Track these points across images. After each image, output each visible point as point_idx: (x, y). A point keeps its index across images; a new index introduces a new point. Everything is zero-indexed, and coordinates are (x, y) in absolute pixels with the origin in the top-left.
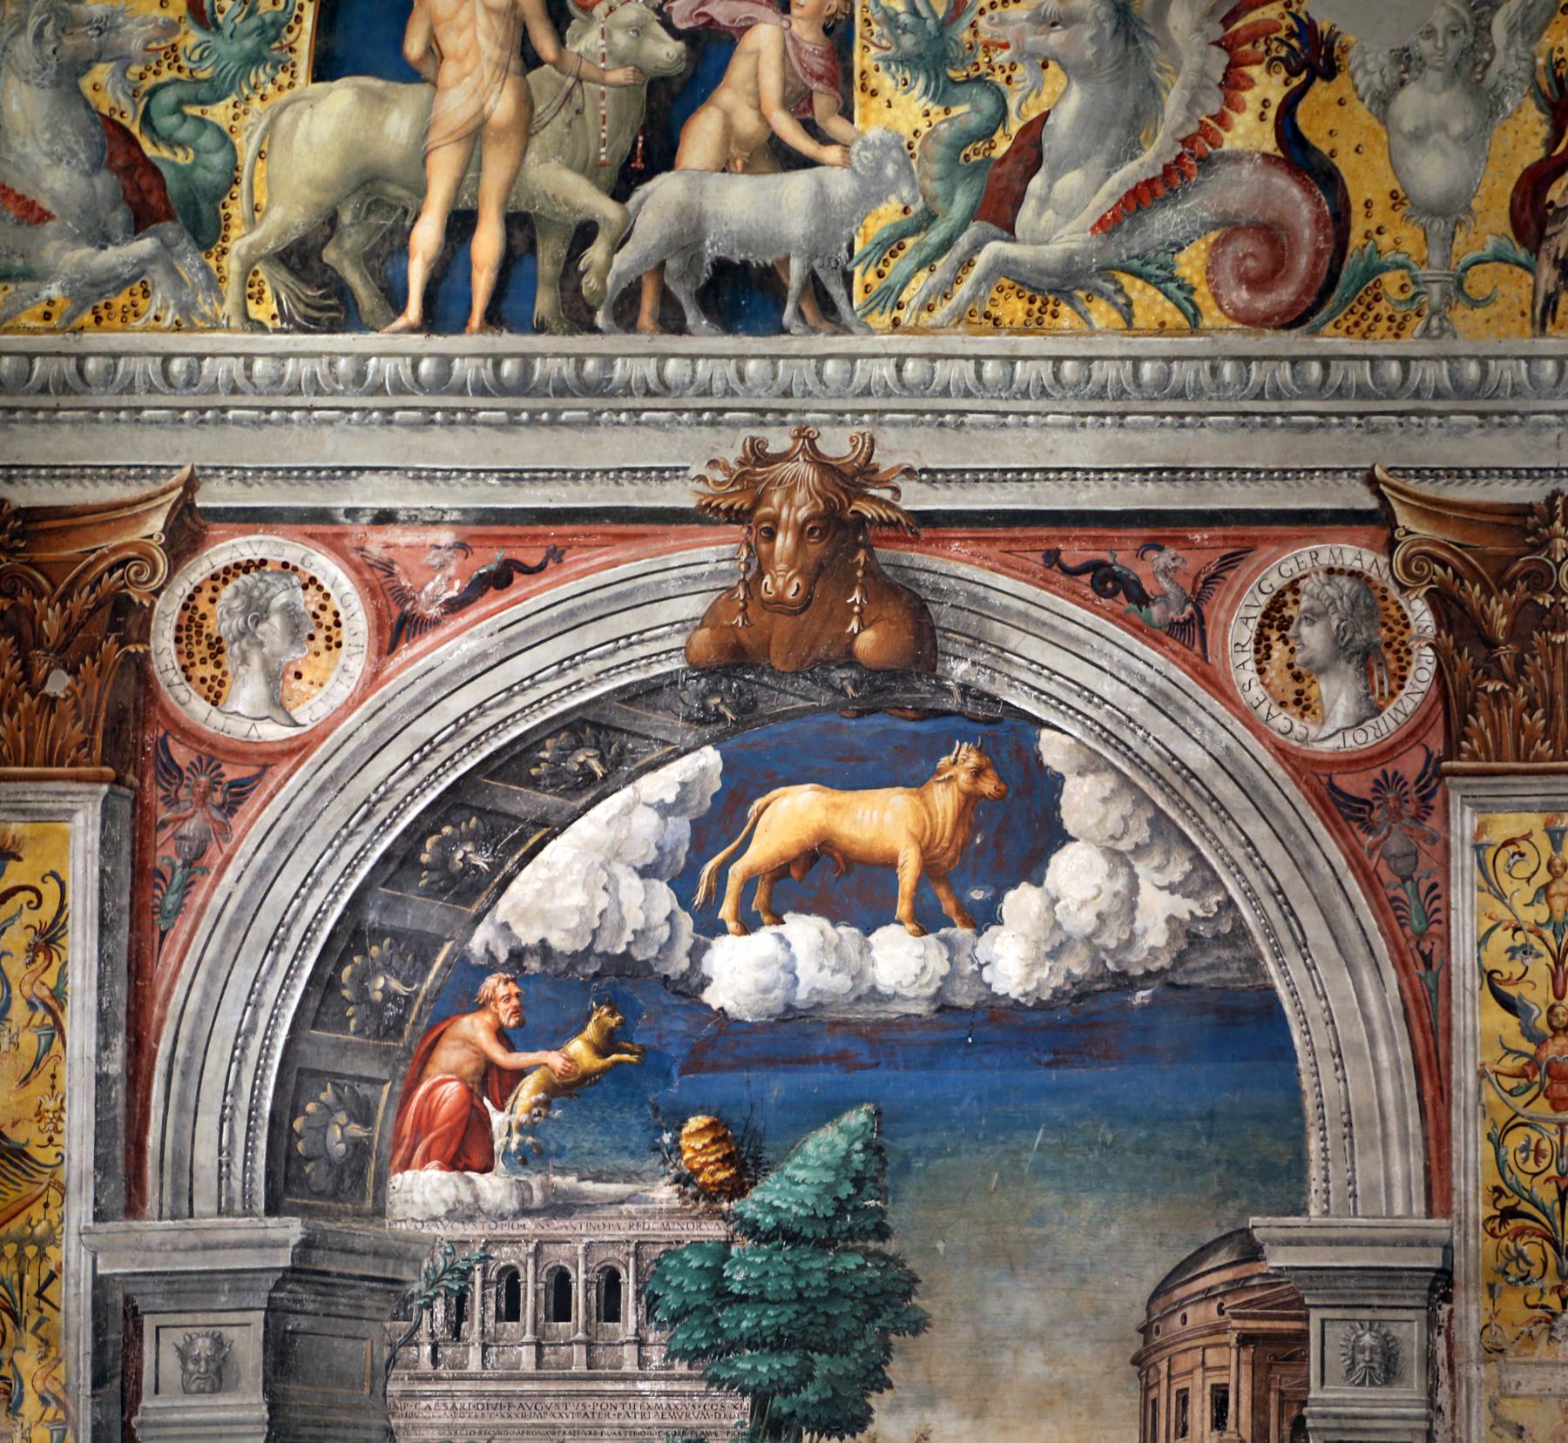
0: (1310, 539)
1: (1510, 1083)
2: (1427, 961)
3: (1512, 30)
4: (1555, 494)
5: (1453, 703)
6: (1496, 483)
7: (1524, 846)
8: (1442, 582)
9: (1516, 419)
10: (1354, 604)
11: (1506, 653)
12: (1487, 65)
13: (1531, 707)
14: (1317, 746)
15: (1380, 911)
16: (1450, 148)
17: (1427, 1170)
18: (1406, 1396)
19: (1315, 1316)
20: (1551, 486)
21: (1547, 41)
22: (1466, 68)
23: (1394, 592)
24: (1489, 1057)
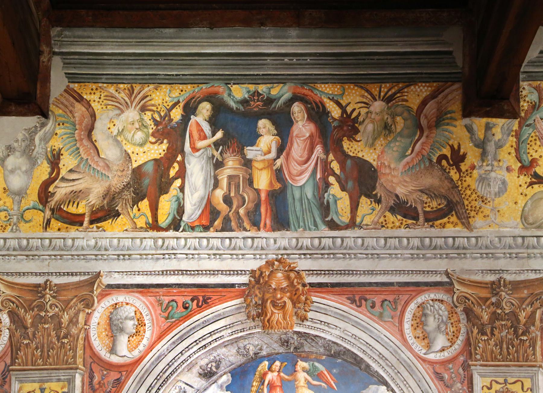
3: (41, 140)
4: (47, 281)
6: (30, 277)
8: (12, 308)
9: (37, 257)
12: (33, 150)
16: (22, 175)
20: (46, 278)
21: (50, 143)
22: (27, 151)
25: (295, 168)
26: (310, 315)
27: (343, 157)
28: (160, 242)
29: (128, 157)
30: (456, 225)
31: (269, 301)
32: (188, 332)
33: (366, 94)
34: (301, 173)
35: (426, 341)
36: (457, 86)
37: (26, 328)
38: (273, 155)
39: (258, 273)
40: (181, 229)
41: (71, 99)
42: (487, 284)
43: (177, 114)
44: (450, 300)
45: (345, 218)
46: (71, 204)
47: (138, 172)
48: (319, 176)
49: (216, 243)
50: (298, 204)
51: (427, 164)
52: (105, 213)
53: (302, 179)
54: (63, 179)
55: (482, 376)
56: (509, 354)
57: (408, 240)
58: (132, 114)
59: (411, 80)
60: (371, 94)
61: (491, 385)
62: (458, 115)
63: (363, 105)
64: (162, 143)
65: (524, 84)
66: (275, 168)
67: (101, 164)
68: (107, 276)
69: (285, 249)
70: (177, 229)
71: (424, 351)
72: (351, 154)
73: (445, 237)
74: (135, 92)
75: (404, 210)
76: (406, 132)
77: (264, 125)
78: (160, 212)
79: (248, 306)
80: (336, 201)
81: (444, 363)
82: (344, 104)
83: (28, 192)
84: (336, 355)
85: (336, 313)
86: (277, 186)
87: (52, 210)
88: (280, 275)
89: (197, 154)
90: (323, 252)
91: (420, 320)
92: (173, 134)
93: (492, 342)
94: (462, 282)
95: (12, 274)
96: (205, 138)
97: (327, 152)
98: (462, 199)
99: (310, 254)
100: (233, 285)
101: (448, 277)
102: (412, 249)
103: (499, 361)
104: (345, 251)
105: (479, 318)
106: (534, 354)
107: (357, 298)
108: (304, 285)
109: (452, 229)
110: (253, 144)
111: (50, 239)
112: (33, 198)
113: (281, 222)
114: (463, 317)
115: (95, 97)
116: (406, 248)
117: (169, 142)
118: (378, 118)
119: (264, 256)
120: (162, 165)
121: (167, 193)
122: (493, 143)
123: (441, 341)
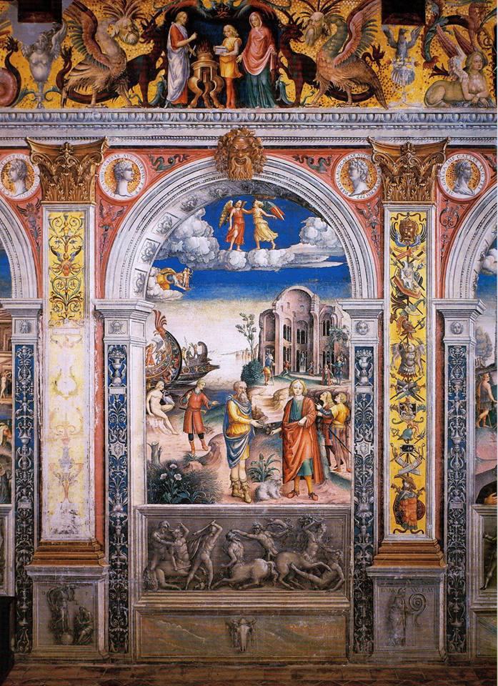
0: (13, 152)
1: (55, 270)
2: (38, 244)
5: (43, 189)
7: (59, 219)
10: (22, 167)
11: (55, 178)
13: (60, 189)
14: (16, 198)
15: (28, 234)
16: (44, 67)
17: (37, 289)
18: (33, 334)
19: (14, 318)
23: (31, 164)
24: (51, 264)
25: (253, 62)
27: (291, 54)
28: (150, 115)
29: (123, 53)
31: (233, 159)
32: (172, 180)
33: (308, 6)
34: (258, 66)
35: (351, 187)
37: (52, 176)
38: (236, 51)
39: (225, 138)
40: (166, 106)
41: (78, 10)
42: (398, 147)
43: (160, 21)
44: (370, 158)
45: (292, 99)
46: (81, 88)
49: (193, 116)
51: (355, 59)
52: (108, 94)
53: (257, 69)
54: (74, 70)
55: (390, 211)
56: (411, 196)
57: (339, 115)
58: (125, 21)
60: (312, 7)
61: (398, 217)
63: (305, 15)
64: (149, 42)
66: (237, 62)
67: (103, 58)
68: (110, 140)
69: (245, 121)
70: (162, 106)
71: (349, 194)
72: (296, 52)
73: (367, 114)
74: (128, 4)
75: (335, 93)
80: (284, 87)
81: (363, 202)
82: (291, 14)
83: (49, 79)
84: (285, 196)
85: (284, 167)
86: (240, 75)
87: (67, 92)
88: (241, 140)
89: (177, 51)
90: (274, 123)
91: (348, 171)
93: (399, 188)
94: (379, 146)
95: (40, 138)
96: (183, 39)
97: (277, 50)
98: (380, 85)
99: (265, 125)
101: (369, 142)
102: (342, 121)
103: (404, 200)
104: (291, 123)
105: (391, 171)
106: (430, 196)
107: (300, 157)
108: (260, 147)
109: (372, 107)
110: (220, 44)
111: (67, 114)
112: (52, 83)
113: (243, 100)
116: (338, 121)
117: (154, 42)
118: (317, 25)
119: (229, 126)
120: (148, 60)
121: (154, 80)
122: (405, 44)
123: (362, 187)
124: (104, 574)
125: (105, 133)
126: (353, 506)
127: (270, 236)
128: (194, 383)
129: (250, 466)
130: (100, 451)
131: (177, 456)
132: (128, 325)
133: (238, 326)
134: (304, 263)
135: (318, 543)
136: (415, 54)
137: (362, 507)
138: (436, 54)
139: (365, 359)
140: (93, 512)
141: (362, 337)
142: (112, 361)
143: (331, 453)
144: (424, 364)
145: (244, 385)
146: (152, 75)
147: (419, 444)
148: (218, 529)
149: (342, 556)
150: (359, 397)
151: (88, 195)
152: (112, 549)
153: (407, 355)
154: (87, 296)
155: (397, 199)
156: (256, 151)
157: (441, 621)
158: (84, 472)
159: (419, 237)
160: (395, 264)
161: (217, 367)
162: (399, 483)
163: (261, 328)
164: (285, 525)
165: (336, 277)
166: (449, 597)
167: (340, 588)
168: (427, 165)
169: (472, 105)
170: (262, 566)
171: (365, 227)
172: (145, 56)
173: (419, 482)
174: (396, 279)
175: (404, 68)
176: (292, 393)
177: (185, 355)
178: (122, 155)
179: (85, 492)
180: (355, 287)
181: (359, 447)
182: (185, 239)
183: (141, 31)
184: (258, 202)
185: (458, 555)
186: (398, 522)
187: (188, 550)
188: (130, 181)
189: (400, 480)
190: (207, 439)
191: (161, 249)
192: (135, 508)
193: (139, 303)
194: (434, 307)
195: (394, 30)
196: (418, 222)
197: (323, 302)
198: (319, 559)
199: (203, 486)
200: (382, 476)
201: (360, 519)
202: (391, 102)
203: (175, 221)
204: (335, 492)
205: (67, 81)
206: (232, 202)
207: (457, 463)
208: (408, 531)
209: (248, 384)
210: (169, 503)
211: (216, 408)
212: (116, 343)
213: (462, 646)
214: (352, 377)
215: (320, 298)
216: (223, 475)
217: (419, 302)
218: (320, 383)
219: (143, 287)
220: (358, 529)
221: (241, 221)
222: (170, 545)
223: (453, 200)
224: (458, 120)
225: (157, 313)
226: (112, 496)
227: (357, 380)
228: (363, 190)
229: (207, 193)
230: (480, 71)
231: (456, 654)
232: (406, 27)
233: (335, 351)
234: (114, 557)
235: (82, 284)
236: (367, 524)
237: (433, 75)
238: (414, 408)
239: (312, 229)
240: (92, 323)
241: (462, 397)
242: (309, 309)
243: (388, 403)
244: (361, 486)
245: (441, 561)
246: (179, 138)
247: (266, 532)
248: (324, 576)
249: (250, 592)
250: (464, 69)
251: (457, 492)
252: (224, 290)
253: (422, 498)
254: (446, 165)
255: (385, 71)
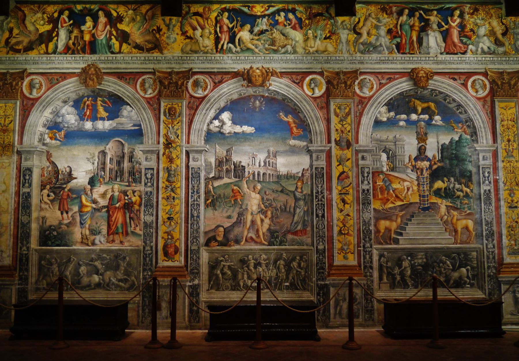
25: (99, 33)
26: (103, 82)
27: (117, 30)
29: (37, 30)
30: (157, 53)
34: (101, 35)
36: (159, 5)
38: (91, 28)
43: (56, 15)
45: (117, 50)
47: (41, 35)
48: (108, 36)
49: (69, 58)
50: (100, 45)
52: (29, 48)
53: (102, 37)
54: (14, 37)
55: (164, 102)
58: (39, 15)
59: (143, 3)
62: (160, 15)
65: (184, 5)
70: (55, 54)
75: (139, 47)
76: (140, 21)
77: (88, 18)
78: (49, 48)
79: (80, 80)
86: (93, 39)
87: (10, 48)
88: (92, 69)
91: (143, 84)
92: (54, 22)
94: (159, 72)
97: (111, 28)
100: (75, 73)
105: (164, 83)
108: (101, 73)
109: (156, 54)
110: (84, 24)
111: (9, 58)
113: (93, 51)
114: (158, 83)
115: (26, 9)
116: (139, 60)
120: (50, 33)
123: (150, 91)
124: (16, 282)
125: (27, 67)
126: (142, 248)
127: (104, 114)
128: (65, 186)
129: (91, 228)
130: (16, 220)
131: (55, 223)
132: (33, 158)
133: (87, 158)
134: (121, 127)
135: (124, 267)
136: (177, 30)
137: (147, 248)
138: (187, 29)
139: (149, 174)
140: (11, 251)
141: (148, 163)
142: (24, 175)
143: (132, 221)
144: (179, 177)
145: (89, 187)
146: (51, 40)
147: (176, 216)
148: (74, 260)
149: (136, 273)
150: (147, 193)
151: (17, 96)
152: (21, 270)
153: (171, 172)
154: (14, 143)
155: (167, 96)
156: (99, 75)
157: (187, 307)
158: (9, 229)
159: (177, 115)
160: (166, 128)
161: (76, 178)
162: (166, 236)
163: (99, 159)
164: (108, 257)
165: (137, 134)
166: (191, 295)
167: (135, 290)
168: (182, 81)
169: (204, 53)
170: (96, 278)
171: (151, 110)
172: (48, 31)
173: (176, 235)
174: (166, 136)
175: (172, 36)
176: (113, 191)
177: (60, 172)
178: (34, 77)
179: (8, 241)
180: (145, 139)
181: (145, 218)
182: (63, 116)
183: (47, 19)
184: (99, 99)
185: (196, 273)
186: (165, 256)
187: (59, 270)
188: (38, 89)
189: (166, 234)
190: (70, 214)
191: (51, 121)
192: (33, 249)
193: (39, 147)
194: (184, 149)
195: (167, 19)
196: (177, 108)
197: (129, 146)
198: (125, 275)
199: (67, 237)
200: (157, 233)
201: (146, 254)
202: (165, 51)
203: (58, 107)
204: (133, 241)
205: (10, 42)
206: (86, 98)
207: (195, 226)
208: (170, 261)
209: (91, 186)
210: (50, 246)
211: (75, 198)
212: (27, 167)
213: (197, 319)
214: (143, 183)
215: (128, 144)
216: (77, 233)
217: (177, 146)
218: (127, 186)
219: (41, 140)
220: (145, 259)
221: (90, 107)
222: (49, 268)
223: (194, 97)
224: (198, 60)
225: (48, 152)
226: (22, 244)
227: (146, 184)
228: (150, 93)
229: (75, 94)
230: (208, 37)
231: (194, 324)
232: (173, 17)
233: (135, 170)
234: (21, 274)
235: (12, 138)
236: (149, 257)
237: (185, 39)
238: (174, 198)
239: (125, 111)
240: (15, 157)
241: (198, 192)
242: (123, 150)
243: (160, 196)
244: (147, 237)
245: (187, 276)
246: (63, 69)
247: (98, 261)
248: (127, 284)
249: (90, 292)
250: (201, 36)
251: (195, 240)
252: (81, 141)
253: (177, 244)
254: (191, 81)
255: (163, 37)
